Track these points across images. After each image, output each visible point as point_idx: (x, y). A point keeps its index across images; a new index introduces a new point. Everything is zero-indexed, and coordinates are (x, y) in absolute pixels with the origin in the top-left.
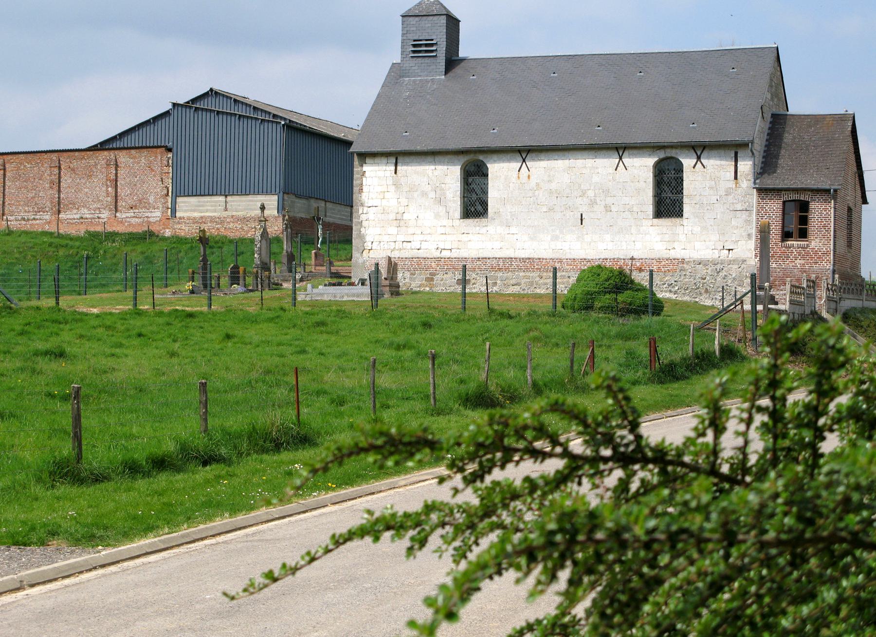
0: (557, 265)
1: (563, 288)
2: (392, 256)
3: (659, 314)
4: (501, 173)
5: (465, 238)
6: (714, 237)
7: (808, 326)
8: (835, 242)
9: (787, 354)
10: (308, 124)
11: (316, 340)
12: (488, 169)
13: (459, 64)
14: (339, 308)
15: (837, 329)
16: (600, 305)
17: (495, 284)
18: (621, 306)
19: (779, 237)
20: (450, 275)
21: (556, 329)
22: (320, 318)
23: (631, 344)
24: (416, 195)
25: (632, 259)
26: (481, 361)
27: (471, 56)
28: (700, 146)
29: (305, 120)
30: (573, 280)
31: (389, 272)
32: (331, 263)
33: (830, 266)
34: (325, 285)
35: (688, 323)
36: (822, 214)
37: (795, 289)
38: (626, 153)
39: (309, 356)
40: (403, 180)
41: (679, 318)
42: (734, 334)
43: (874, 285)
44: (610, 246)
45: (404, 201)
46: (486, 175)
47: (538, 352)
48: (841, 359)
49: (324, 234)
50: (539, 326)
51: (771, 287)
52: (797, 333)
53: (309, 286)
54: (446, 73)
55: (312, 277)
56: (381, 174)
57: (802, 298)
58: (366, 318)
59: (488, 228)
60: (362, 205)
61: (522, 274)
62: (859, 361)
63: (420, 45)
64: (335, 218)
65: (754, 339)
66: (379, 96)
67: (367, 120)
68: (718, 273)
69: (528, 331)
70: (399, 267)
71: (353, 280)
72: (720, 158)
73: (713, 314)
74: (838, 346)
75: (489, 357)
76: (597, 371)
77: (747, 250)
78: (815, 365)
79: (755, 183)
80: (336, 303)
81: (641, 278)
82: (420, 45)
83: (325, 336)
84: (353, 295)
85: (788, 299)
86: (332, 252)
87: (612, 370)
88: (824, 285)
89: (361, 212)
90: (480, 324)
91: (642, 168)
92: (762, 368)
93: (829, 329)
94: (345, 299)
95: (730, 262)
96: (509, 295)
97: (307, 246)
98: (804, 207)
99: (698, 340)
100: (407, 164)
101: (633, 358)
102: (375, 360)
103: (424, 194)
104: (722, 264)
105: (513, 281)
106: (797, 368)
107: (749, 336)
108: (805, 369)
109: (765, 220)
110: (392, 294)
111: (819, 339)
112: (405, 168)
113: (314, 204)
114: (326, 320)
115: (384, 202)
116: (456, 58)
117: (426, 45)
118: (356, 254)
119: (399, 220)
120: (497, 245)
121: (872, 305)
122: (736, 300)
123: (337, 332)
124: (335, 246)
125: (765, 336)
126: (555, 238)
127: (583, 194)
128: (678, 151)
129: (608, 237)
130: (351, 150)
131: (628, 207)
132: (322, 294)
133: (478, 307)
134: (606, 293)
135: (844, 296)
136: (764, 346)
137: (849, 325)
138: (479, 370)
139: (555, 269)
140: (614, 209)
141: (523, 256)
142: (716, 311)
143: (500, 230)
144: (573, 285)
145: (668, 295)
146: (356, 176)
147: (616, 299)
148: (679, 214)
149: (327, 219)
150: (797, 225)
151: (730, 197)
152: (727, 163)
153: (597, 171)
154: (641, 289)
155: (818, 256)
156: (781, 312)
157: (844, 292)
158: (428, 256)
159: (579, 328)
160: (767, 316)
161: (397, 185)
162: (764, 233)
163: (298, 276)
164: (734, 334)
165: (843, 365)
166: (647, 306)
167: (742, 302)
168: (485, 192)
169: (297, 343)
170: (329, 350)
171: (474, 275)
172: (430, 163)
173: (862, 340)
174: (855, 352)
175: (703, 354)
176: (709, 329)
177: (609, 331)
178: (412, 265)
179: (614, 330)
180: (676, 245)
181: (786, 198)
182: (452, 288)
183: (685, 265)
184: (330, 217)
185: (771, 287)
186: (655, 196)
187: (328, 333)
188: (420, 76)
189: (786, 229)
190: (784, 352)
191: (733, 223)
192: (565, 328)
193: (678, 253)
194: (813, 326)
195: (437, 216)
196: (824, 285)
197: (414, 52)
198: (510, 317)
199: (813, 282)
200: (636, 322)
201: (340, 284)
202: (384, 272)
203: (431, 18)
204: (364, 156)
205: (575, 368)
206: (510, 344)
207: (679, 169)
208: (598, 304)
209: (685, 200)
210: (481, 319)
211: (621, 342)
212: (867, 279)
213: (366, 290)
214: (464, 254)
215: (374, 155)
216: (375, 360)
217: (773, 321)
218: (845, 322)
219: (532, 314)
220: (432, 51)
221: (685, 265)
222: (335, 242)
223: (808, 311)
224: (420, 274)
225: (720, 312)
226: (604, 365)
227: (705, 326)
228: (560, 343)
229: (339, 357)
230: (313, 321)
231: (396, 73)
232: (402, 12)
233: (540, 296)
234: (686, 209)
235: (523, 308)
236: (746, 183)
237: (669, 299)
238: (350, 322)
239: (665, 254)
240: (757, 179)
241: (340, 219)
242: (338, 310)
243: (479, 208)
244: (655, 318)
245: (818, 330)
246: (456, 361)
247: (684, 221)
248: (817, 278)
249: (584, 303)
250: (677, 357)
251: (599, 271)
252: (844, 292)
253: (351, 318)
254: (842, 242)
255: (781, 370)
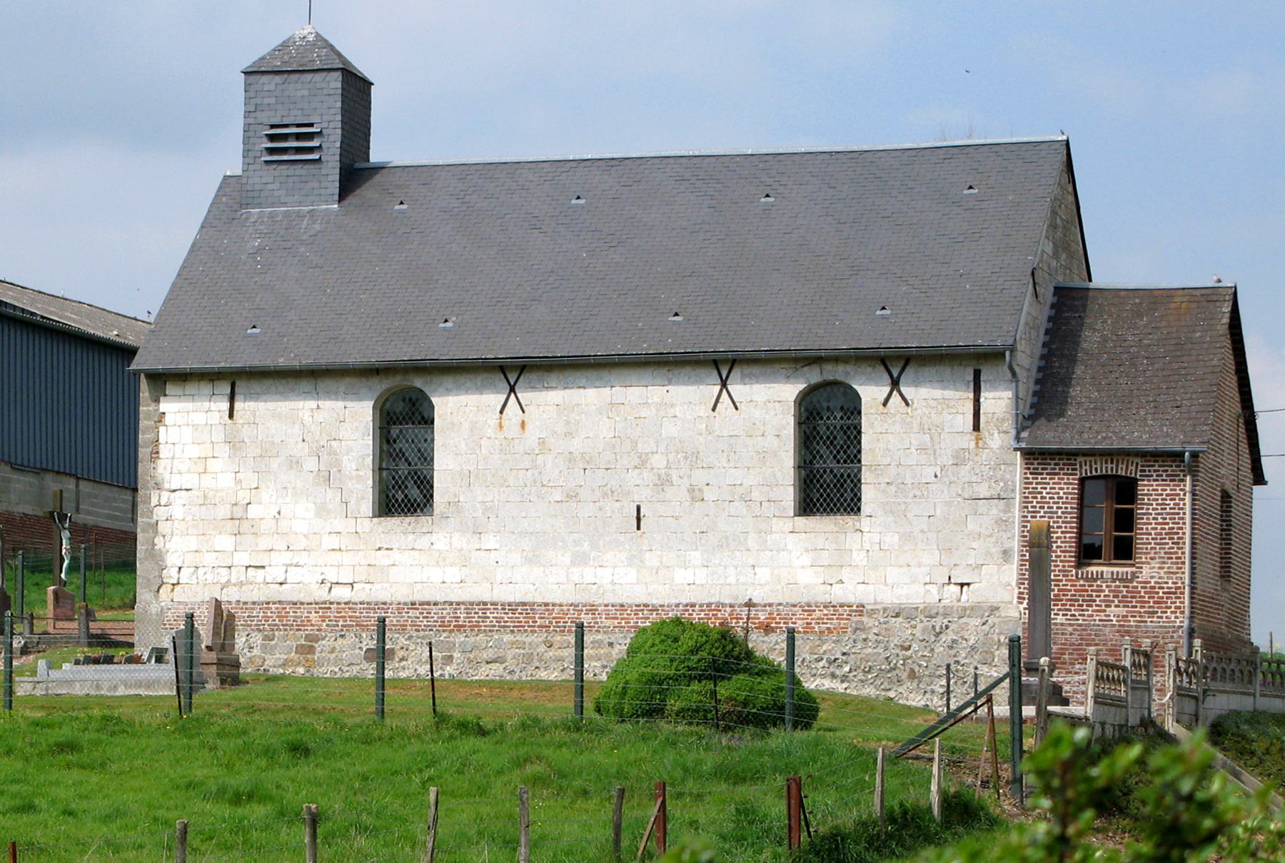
0: (586, 619)
1: (597, 670)
2: (224, 598)
3: (807, 726)
4: (460, 415)
5: (382, 558)
6: (930, 557)
7: (1135, 751)
8: (1193, 569)
9: (1089, 814)
10: (39, 309)
11: (57, 783)
12: (433, 407)
13: (370, 177)
14: (107, 712)
15: (1197, 758)
16: (678, 705)
17: (449, 659)
18: (724, 708)
19: (1071, 558)
20: (350, 639)
21: (583, 759)
22: (63, 734)
23: (746, 791)
24: (275, 463)
25: (750, 604)
26: (419, 829)
27: (397, 160)
28: (898, 357)
29: (33, 302)
30: (620, 650)
31: (216, 633)
32: (89, 615)
33: (1183, 621)
34: (77, 662)
35: (872, 745)
36: (1165, 506)
37: (1107, 671)
38: (736, 373)
39: (41, 817)
40: (246, 433)
41: (851, 734)
42: (973, 770)
43: (1279, 663)
44: (701, 576)
45: (249, 478)
46: (430, 422)
47: (543, 808)
48: (1208, 823)
49: (73, 549)
50: (548, 752)
51: (1052, 667)
52: (1111, 766)
53: (42, 664)
54: (342, 197)
55: (49, 644)
56: (200, 418)
57: (1122, 691)
58: (167, 735)
59: (434, 538)
60: (158, 486)
61: (507, 638)
62: (1246, 828)
63: (285, 137)
64: (98, 515)
65: (1017, 780)
66: (195, 248)
67: (168, 300)
68: (938, 634)
69: (520, 763)
70: (239, 623)
71: (137, 651)
72: (942, 383)
73: (926, 726)
74: (1200, 795)
75: (435, 820)
76: (672, 850)
77: (1000, 585)
78: (1150, 837)
79: (1018, 439)
80: (102, 701)
81: (769, 647)
82: (285, 137)
83: (76, 774)
84: (139, 684)
85: (1090, 693)
86: (93, 590)
87: (706, 848)
88: (1169, 662)
89: (154, 501)
90: (416, 746)
91: (771, 404)
92: (1034, 843)
93: (1180, 758)
94: (121, 691)
95: (964, 612)
96: (481, 684)
97: (38, 577)
98: (1125, 491)
99: (893, 783)
100: (255, 396)
101: (751, 823)
102: (186, 826)
103: (294, 463)
104: (945, 615)
105: (489, 654)
106: (1110, 845)
107: (1006, 774)
108: (1127, 846)
109: (1041, 519)
110: (223, 682)
111: (1158, 781)
112: (251, 405)
113: (52, 484)
114: (78, 738)
115: (207, 481)
116: (364, 165)
117: (299, 137)
118: (143, 595)
119: (238, 521)
120: (453, 574)
121: (1276, 705)
122: (978, 696)
123: (103, 765)
124: (98, 576)
125: (1041, 773)
126: (580, 559)
127: (643, 463)
128: (849, 368)
129: (696, 556)
130: (133, 367)
131: (740, 490)
132: (70, 683)
133: (411, 710)
134: (691, 678)
135: (1213, 685)
136: (1037, 796)
137: (1224, 749)
138: (413, 848)
139: (580, 627)
140: (709, 495)
141: (512, 600)
142: (933, 720)
143: (459, 541)
144: (620, 662)
145: (827, 684)
146: (143, 423)
147: (714, 693)
148: (851, 504)
149: (82, 518)
150: (1109, 532)
151: (964, 471)
152: (958, 394)
153: (671, 412)
154: (768, 670)
155: (1158, 599)
156: (1074, 722)
157: (1214, 678)
158: (302, 597)
159: (632, 757)
160: (1044, 729)
161: (234, 443)
162: (1037, 549)
163: (18, 643)
164: (973, 770)
165: (1210, 838)
166: (782, 708)
167: (990, 700)
168: (428, 459)
169: (15, 788)
170: (84, 804)
171: (403, 641)
172: (306, 395)
173: (1253, 782)
174: (1237, 809)
175: (905, 812)
176: (917, 758)
177: (699, 762)
178: (267, 618)
179: (710, 761)
180: (845, 574)
181: (1086, 471)
182: (355, 669)
183: (865, 619)
184: (88, 513)
185: (1052, 667)
186: (799, 467)
187: (82, 767)
188: (284, 204)
189: (1086, 540)
190: (1081, 809)
191: (971, 526)
192: (603, 756)
193: (850, 591)
194: (1146, 751)
195: (322, 511)
196: (1169, 662)
197: (271, 151)
198: (482, 732)
199: (1146, 655)
200: (759, 744)
201: (109, 660)
202: (205, 635)
203: (308, 76)
204: (162, 380)
205: (625, 843)
206: (483, 791)
207: (853, 408)
208: (674, 704)
209: (866, 476)
210: (419, 737)
211: (724, 786)
212: (1264, 648)
213: (167, 672)
214: (379, 592)
215: (183, 377)
216: (186, 826)
217: (1057, 741)
218: (1215, 743)
219: (530, 725)
220: (311, 150)
221: (865, 619)
222: (98, 567)
223: (1134, 720)
224: (285, 638)
225: (942, 722)
226: (687, 837)
227: (908, 752)
228: (591, 788)
229: (107, 819)
230: (51, 741)
231: (233, 199)
232: (246, 63)
233: (548, 686)
234: (868, 494)
235: (509, 711)
236: (1000, 437)
237: (831, 694)
238: (131, 743)
239: (821, 594)
240: (1024, 429)
241: (109, 517)
242: (104, 718)
243: (414, 493)
244: (800, 735)
245: (1157, 760)
246: (363, 829)
247: (864, 523)
248: (1154, 646)
249: (644, 701)
250: (847, 819)
251: (676, 632)
252: (1214, 678)
253: (134, 735)
254: (1210, 568)
255: (1075, 848)
